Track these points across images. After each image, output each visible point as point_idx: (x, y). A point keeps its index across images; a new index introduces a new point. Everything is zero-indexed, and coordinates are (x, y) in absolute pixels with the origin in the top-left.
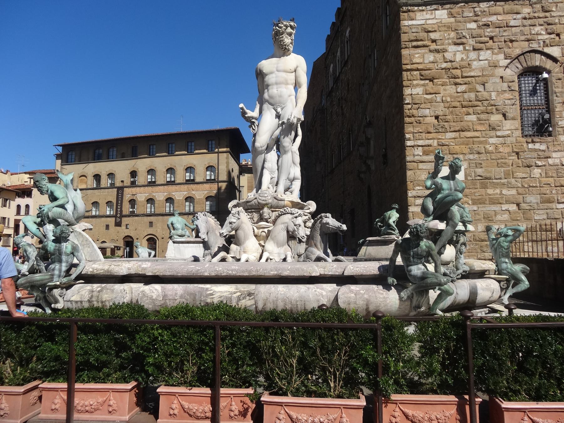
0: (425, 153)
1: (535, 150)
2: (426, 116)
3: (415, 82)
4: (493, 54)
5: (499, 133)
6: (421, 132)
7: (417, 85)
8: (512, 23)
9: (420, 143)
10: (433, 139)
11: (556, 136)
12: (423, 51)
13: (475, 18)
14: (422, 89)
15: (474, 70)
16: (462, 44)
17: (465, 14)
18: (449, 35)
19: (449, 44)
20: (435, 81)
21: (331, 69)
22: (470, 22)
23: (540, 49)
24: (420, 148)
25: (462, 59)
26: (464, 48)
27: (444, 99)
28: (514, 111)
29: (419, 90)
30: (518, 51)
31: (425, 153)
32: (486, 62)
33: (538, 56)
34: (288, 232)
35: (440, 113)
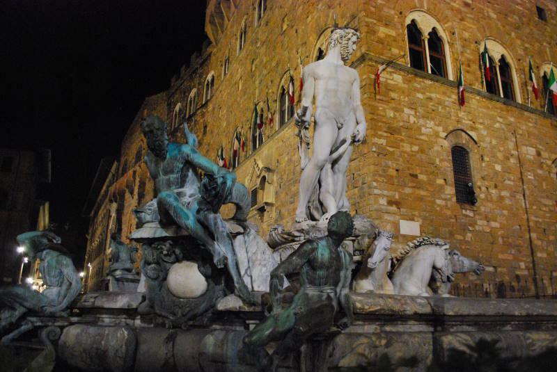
0: (390, 203)
1: (467, 216)
2: (389, 167)
3: (380, 133)
4: (435, 125)
5: (443, 196)
6: (386, 183)
7: (380, 137)
8: (447, 103)
9: (385, 192)
10: (395, 191)
11: (478, 208)
12: (385, 106)
13: (422, 91)
14: (385, 141)
15: (423, 134)
16: (415, 109)
17: (415, 85)
18: (404, 98)
19: (404, 106)
20: (396, 136)
21: (177, 108)
22: (418, 92)
23: (465, 130)
24: (385, 199)
25: (414, 122)
26: (416, 113)
27: (403, 154)
28: (451, 177)
29: (383, 141)
30: (451, 128)
31: (390, 203)
32: (431, 130)
33: (463, 134)
34: (434, 267)
35: (401, 168)
